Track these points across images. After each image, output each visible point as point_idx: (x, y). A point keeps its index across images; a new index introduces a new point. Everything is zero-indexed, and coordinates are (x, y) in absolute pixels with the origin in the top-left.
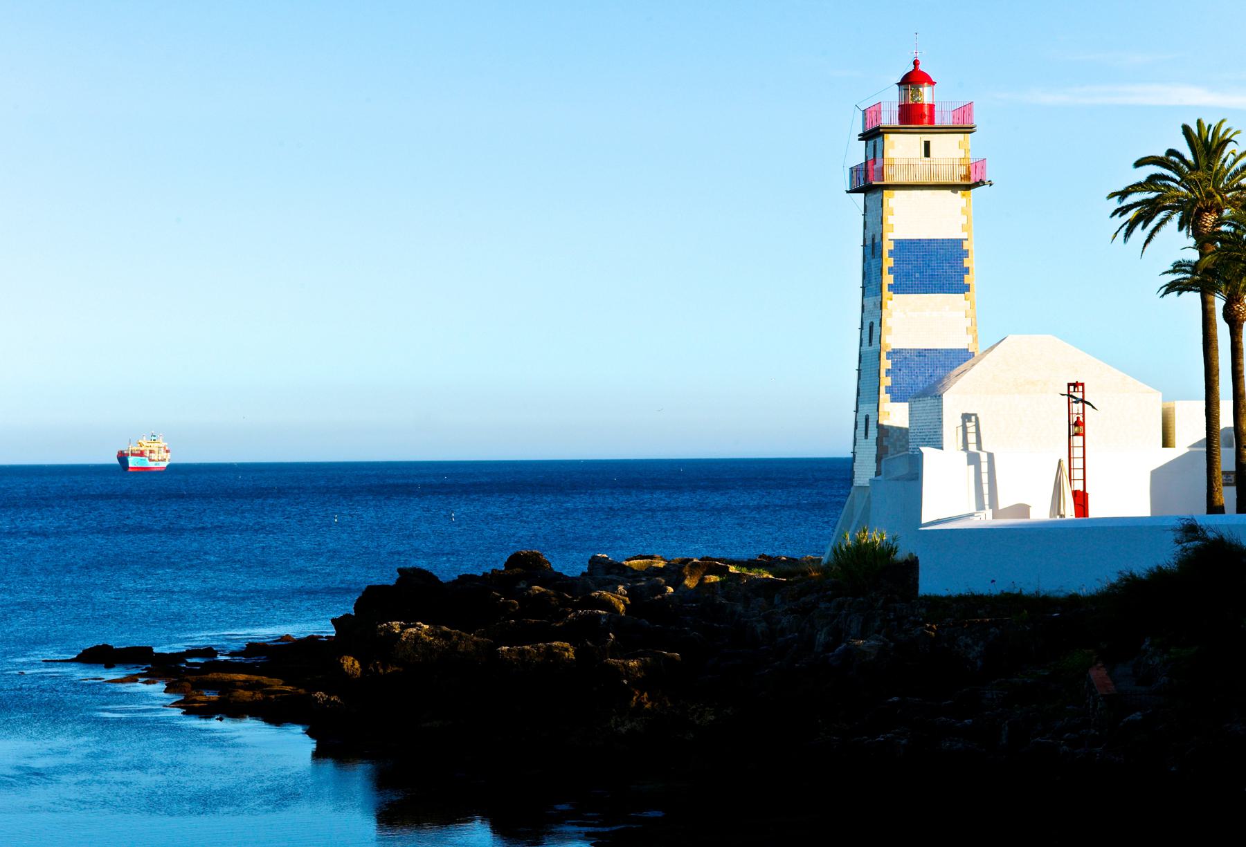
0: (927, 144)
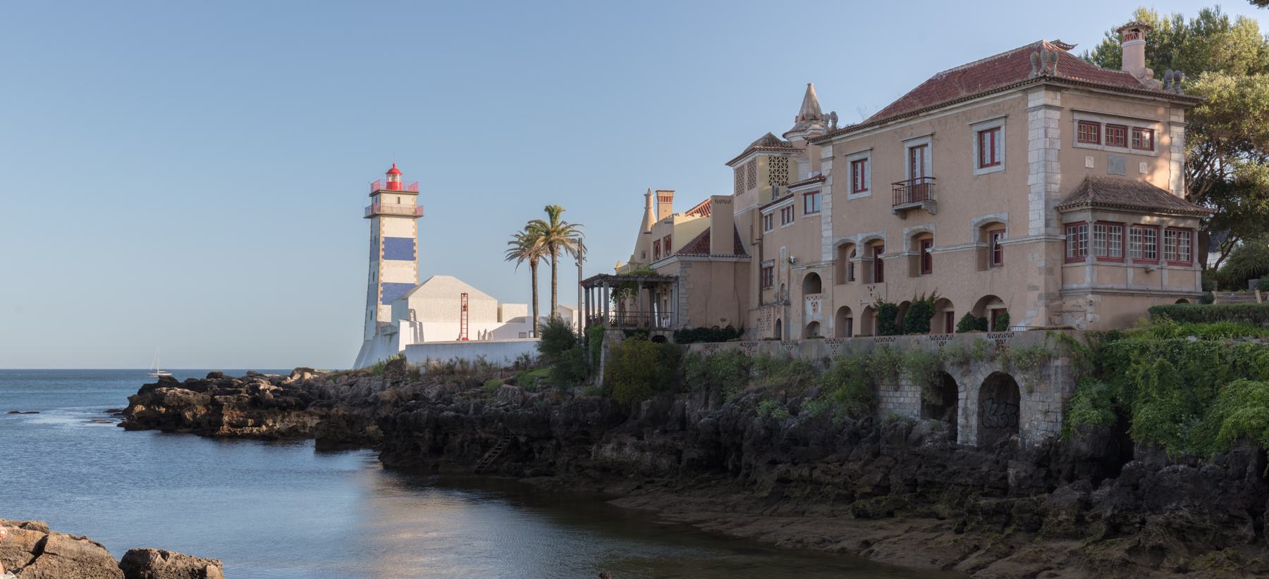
0: (399, 198)
